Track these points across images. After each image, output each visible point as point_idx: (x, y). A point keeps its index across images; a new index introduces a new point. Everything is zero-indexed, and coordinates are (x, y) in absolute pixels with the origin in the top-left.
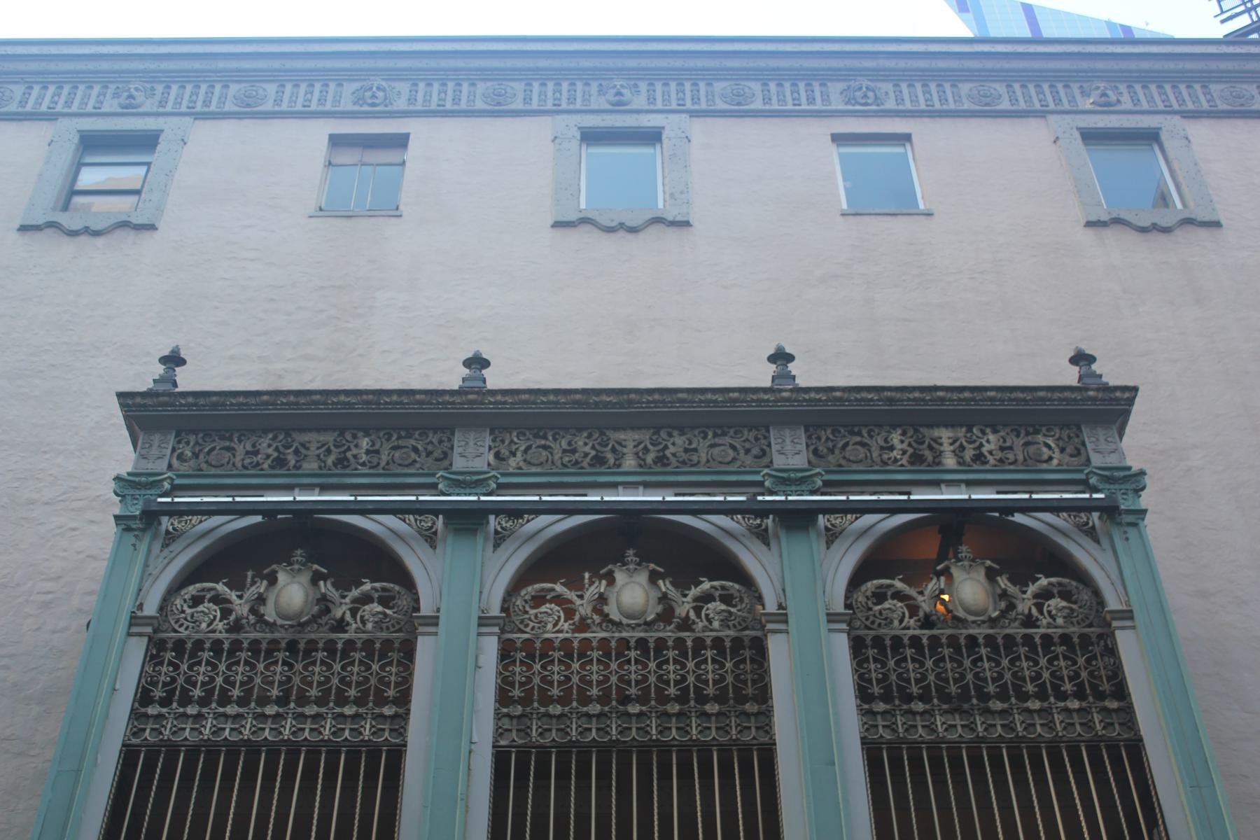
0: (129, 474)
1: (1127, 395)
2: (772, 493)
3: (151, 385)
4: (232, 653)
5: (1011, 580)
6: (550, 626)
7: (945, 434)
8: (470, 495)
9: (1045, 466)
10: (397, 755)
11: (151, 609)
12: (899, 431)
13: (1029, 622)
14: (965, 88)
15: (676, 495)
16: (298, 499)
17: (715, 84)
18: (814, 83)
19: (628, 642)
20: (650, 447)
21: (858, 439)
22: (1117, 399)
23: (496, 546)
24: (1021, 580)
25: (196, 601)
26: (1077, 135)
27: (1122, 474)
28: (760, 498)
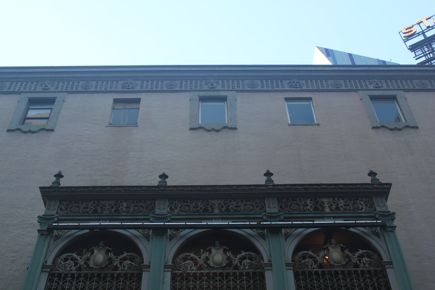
0: (43, 215)
1: (388, 186)
2: (266, 221)
3: (51, 184)
4: (78, 278)
5: (350, 251)
6: (189, 268)
7: (325, 200)
8: (161, 222)
9: (360, 211)
11: (50, 263)
12: (310, 200)
13: (356, 266)
14: (330, 82)
15: (233, 222)
16: (102, 224)
17: (328, 81)
18: (278, 81)
19: (338, 272)
20: (224, 205)
21: (296, 202)
22: (384, 188)
23: (170, 240)
24: (353, 251)
25: (66, 260)
26: (368, 97)
27: (387, 214)
28: (262, 223)
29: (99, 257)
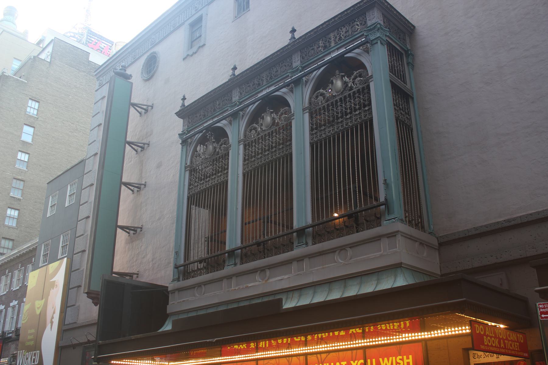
10: (371, 120)
11: (307, 105)
23: (293, 92)
25: (317, 97)
29: (268, 119)
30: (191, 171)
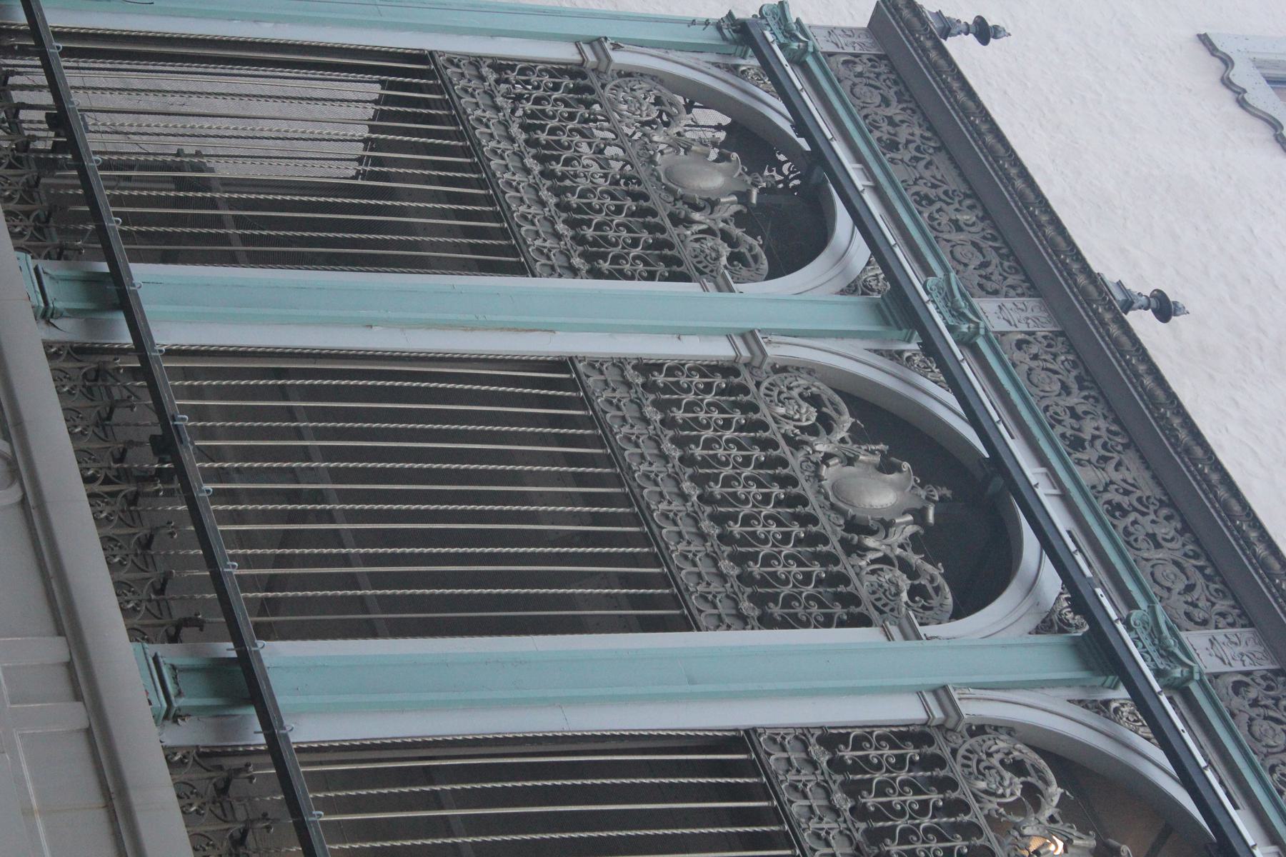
0: (798, 22)
11: (974, 709)
15: (1069, 532)
25: (1018, 768)
28: (1099, 591)
30: (576, 71)
